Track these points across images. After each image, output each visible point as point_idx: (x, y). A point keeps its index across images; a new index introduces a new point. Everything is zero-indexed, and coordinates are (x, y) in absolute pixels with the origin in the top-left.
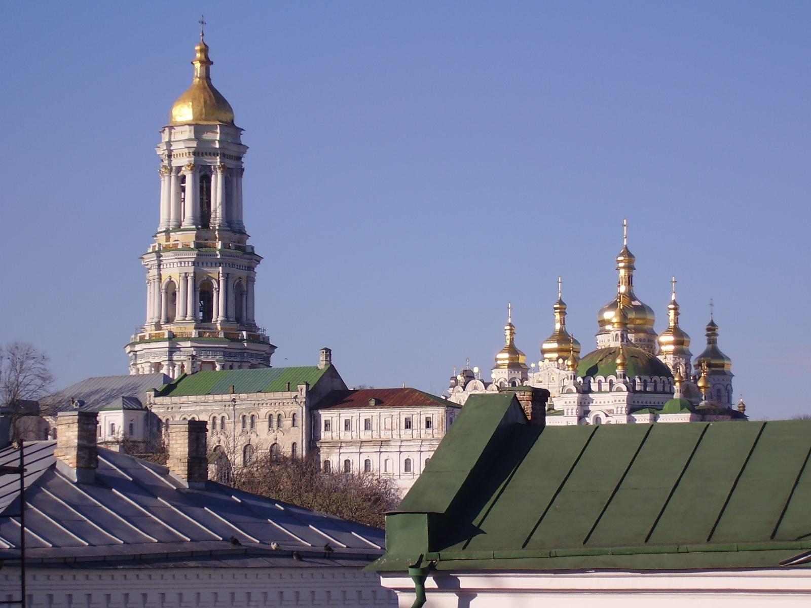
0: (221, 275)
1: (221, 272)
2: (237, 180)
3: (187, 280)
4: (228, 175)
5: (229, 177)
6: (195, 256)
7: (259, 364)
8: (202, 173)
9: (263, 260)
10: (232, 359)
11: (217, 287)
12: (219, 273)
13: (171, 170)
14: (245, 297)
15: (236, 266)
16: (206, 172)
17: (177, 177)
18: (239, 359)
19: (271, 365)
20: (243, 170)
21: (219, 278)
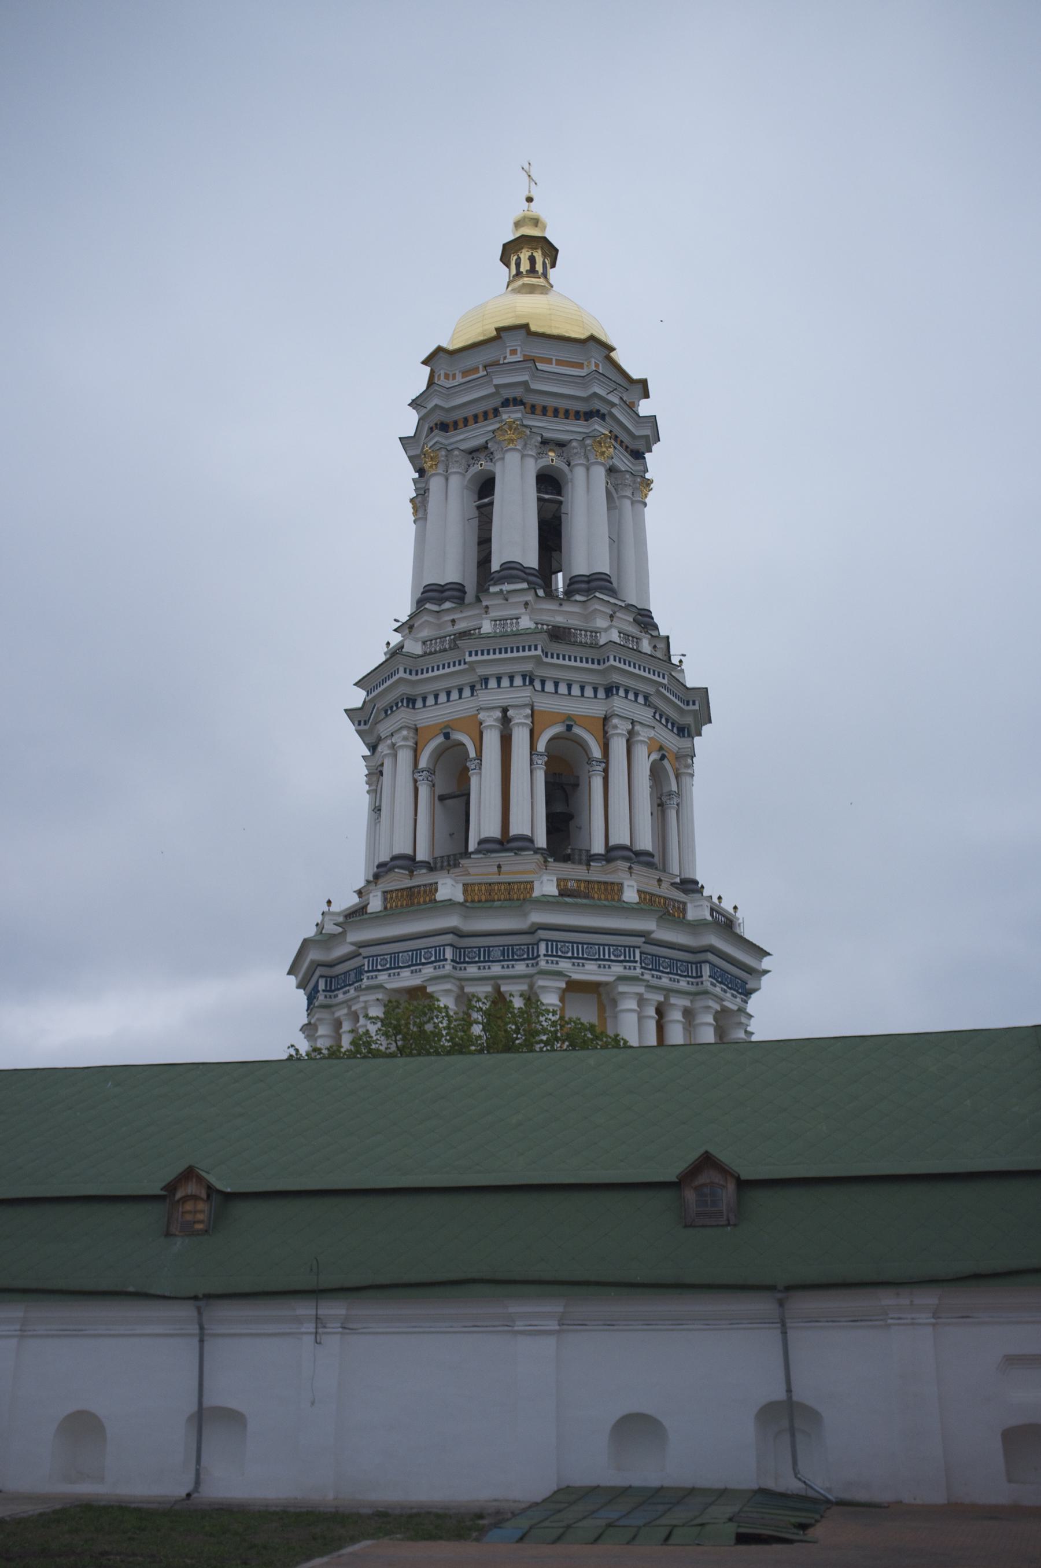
8: (543, 462)
9: (710, 724)
10: (665, 981)
18: (683, 984)
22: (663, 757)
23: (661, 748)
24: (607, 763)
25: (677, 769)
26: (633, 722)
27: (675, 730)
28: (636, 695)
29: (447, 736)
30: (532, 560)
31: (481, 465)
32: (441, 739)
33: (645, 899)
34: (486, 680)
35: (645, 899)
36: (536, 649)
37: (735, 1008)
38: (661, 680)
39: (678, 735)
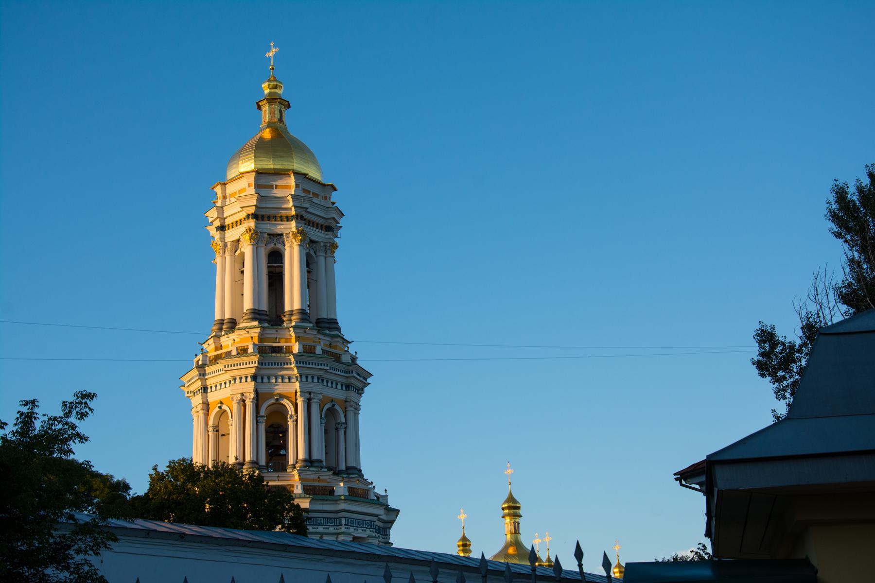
0: (298, 394)
1: (298, 390)
2: (325, 258)
3: (245, 406)
4: (312, 252)
5: (313, 254)
6: (256, 365)
7: (368, 537)
8: (271, 246)
9: (372, 377)
11: (293, 413)
12: (296, 392)
13: (225, 245)
14: (342, 432)
15: (325, 382)
16: (275, 244)
17: (234, 261)
18: (332, 530)
19: (391, 541)
20: (334, 246)
21: (296, 400)
22: (334, 405)
23: (332, 401)
24: (297, 417)
25: (346, 408)
26: (310, 393)
27: (344, 388)
28: (313, 378)
29: (220, 407)
30: (264, 306)
31: (240, 250)
32: (217, 409)
33: (307, 489)
34: (235, 379)
35: (307, 489)
36: (255, 363)
37: (367, 536)
38: (326, 368)
39: (346, 390)
